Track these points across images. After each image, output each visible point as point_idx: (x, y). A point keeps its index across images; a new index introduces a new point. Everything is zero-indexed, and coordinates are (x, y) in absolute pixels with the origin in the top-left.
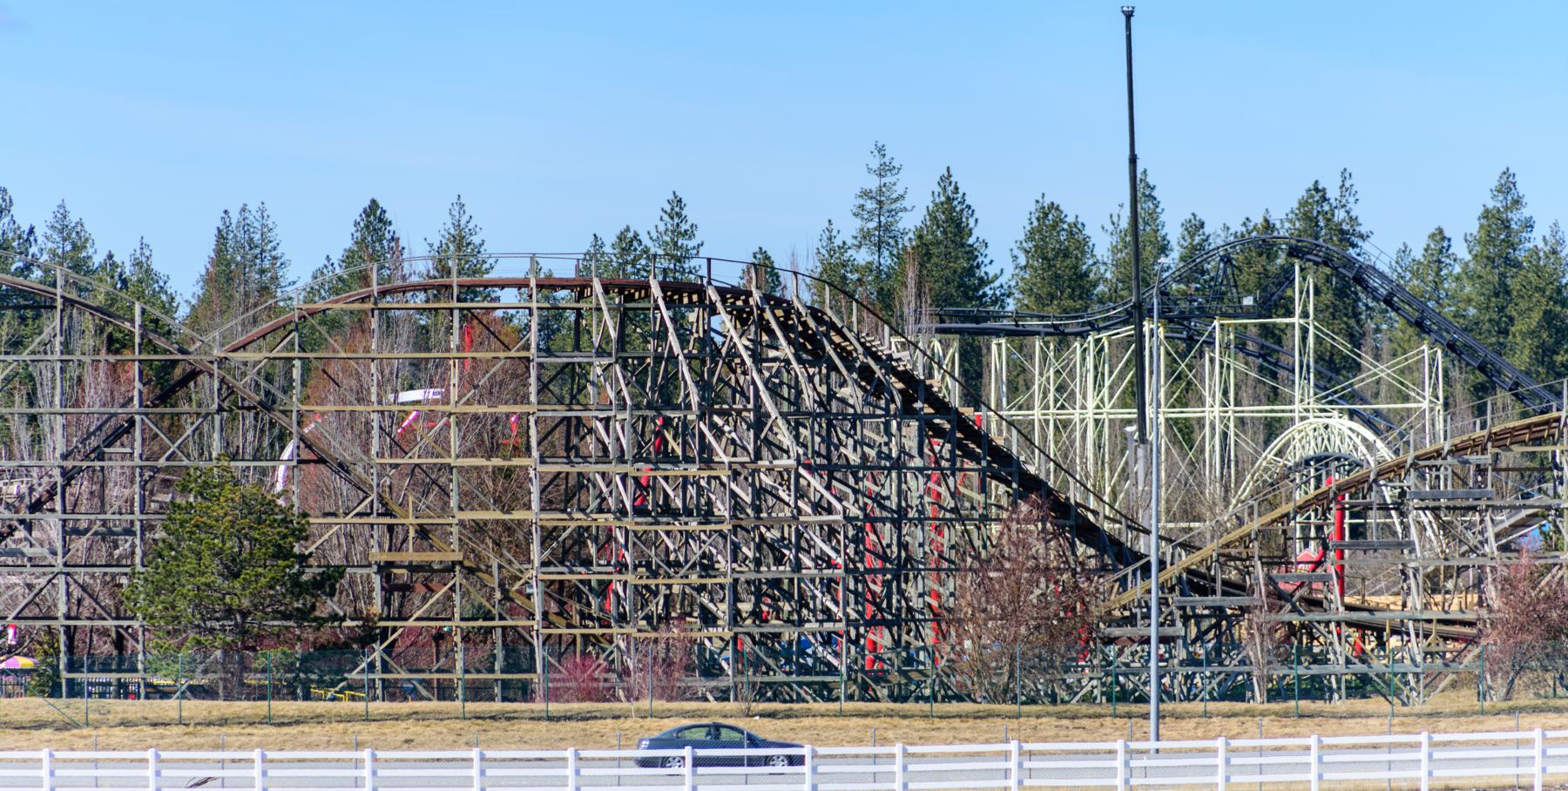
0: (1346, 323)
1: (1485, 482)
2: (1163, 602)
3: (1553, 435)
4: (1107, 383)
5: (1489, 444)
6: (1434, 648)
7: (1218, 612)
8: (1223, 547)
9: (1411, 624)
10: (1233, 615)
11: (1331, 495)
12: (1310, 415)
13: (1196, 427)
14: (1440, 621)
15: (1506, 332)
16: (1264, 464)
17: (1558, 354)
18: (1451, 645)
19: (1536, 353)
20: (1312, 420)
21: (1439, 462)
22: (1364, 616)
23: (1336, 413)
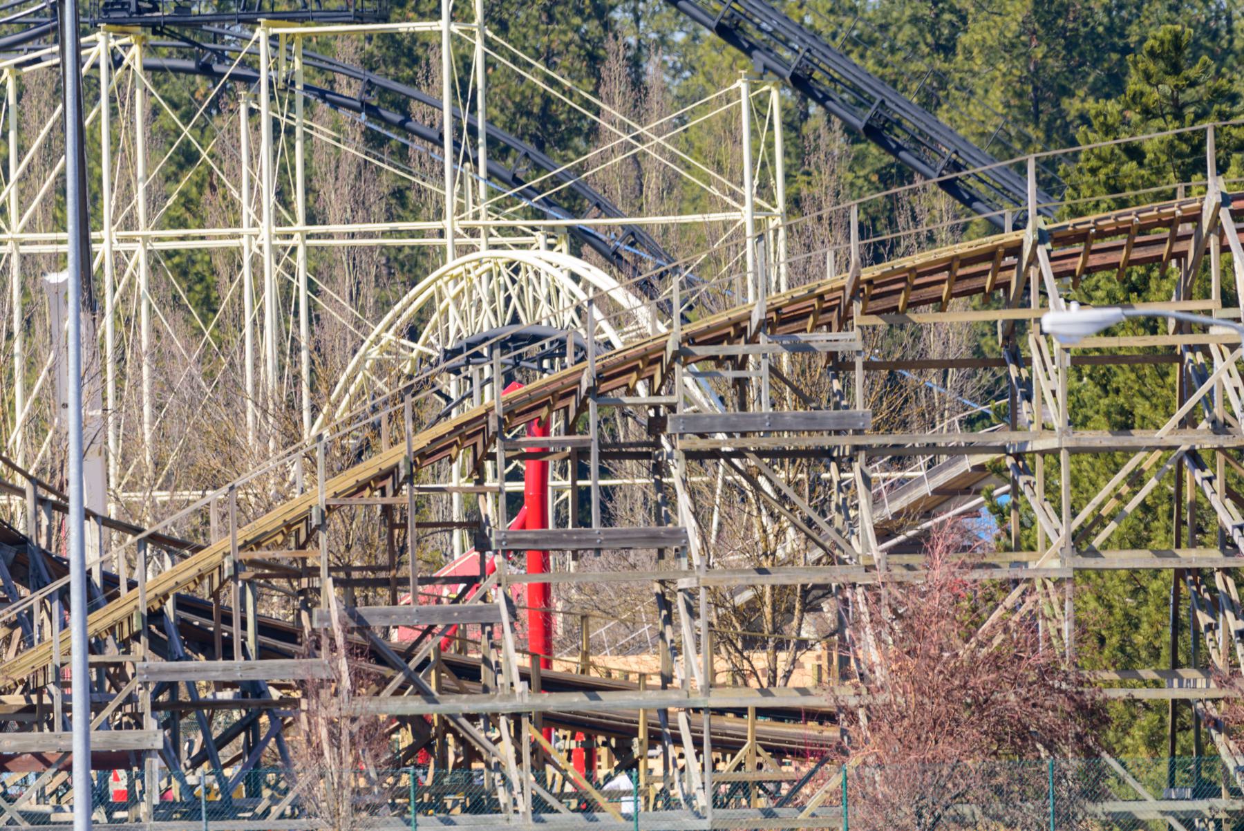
0: (577, 29)
1: (846, 392)
2: (110, 675)
3: (1006, 286)
4: (14, 175)
5: (857, 307)
6: (749, 774)
7: (252, 691)
8: (245, 546)
9: (682, 719)
10: (283, 702)
11: (493, 424)
12: (481, 241)
13: (224, 271)
14: (761, 712)
15: (946, 48)
16: (375, 353)
17: (1072, 95)
18: (791, 768)
19: (1020, 95)
20: (484, 253)
21: (739, 349)
22: (575, 701)
23: (540, 238)
